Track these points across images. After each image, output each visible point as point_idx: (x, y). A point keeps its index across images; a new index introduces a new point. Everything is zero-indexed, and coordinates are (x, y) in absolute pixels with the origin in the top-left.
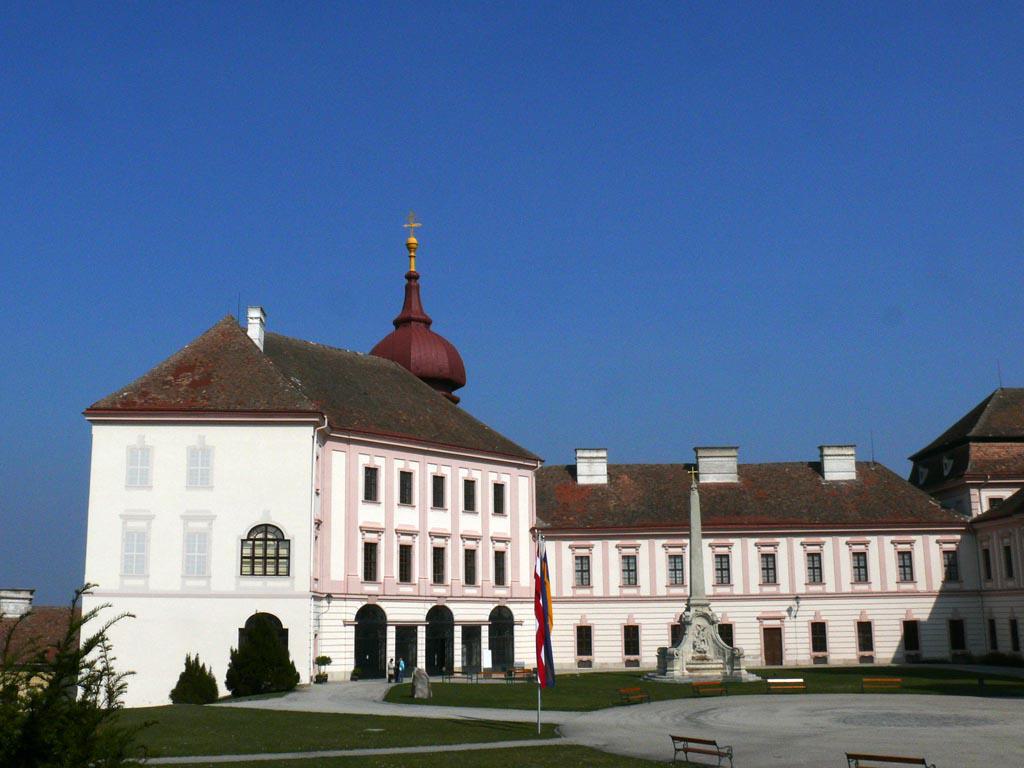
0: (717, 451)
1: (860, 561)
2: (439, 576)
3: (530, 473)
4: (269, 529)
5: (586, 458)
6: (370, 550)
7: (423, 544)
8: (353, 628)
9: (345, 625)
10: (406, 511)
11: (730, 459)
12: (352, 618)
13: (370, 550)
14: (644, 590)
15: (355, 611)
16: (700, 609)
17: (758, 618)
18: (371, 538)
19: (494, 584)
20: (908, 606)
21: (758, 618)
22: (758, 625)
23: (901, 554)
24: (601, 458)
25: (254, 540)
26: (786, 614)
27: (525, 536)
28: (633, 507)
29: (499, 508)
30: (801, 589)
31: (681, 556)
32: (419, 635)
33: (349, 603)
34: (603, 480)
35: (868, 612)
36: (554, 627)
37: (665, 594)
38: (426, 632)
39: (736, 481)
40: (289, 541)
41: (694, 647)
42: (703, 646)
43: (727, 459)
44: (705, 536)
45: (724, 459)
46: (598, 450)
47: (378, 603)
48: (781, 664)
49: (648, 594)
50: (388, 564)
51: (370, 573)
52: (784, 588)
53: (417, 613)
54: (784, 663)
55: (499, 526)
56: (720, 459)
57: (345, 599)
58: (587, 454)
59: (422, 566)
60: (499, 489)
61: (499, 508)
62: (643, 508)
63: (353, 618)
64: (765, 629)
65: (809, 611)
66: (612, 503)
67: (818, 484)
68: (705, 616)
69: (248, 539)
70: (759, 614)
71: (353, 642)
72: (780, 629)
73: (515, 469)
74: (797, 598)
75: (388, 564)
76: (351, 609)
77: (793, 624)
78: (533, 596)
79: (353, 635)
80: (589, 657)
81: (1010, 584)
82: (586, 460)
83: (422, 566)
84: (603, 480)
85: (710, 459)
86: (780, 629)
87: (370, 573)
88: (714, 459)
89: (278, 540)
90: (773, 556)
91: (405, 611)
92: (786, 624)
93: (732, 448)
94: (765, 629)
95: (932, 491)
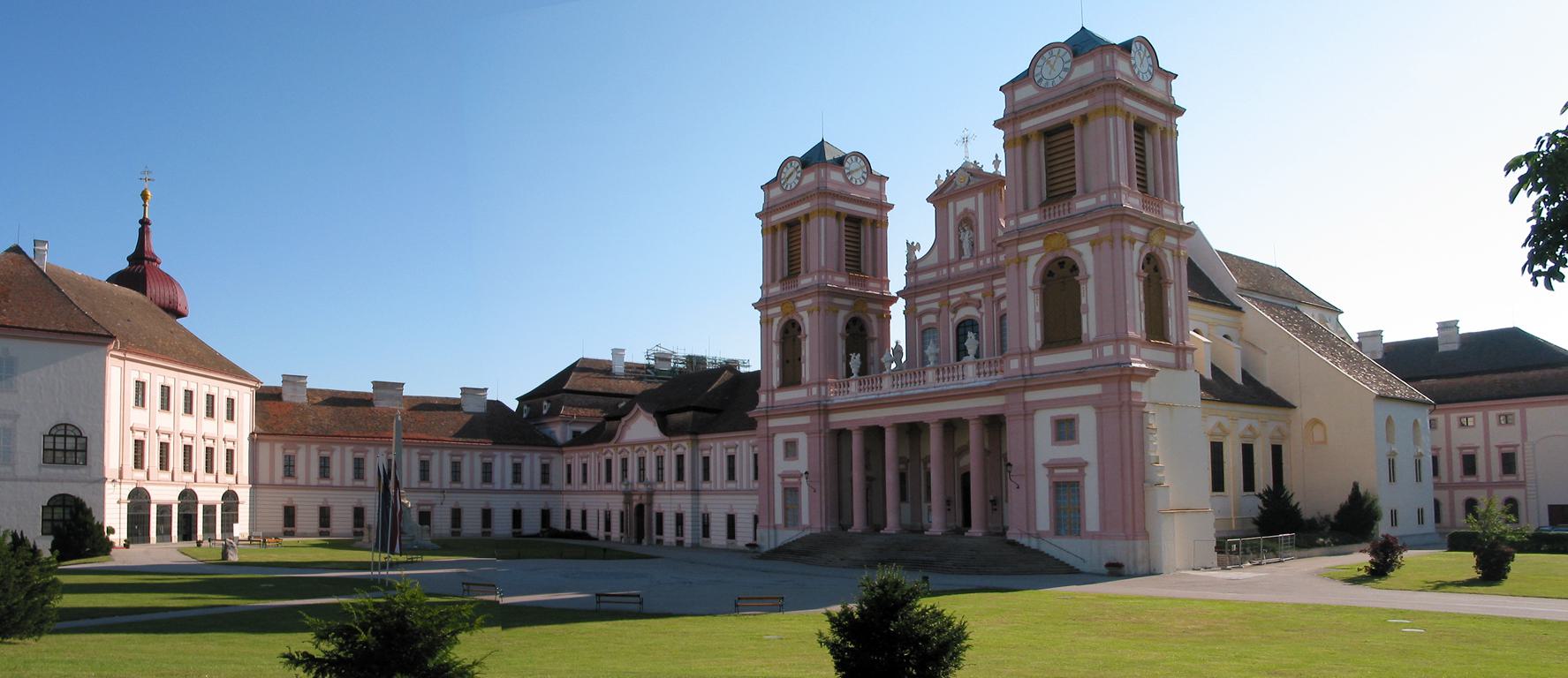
2: (187, 467)
4: (68, 427)
6: (139, 445)
10: (165, 415)
12: (125, 497)
13: (139, 445)
25: (55, 436)
29: (230, 416)
36: (299, 511)
40: (86, 438)
47: (144, 487)
49: (338, 485)
50: (152, 456)
51: (139, 463)
52: (435, 485)
55: (229, 429)
59: (176, 459)
60: (231, 402)
61: (230, 416)
65: (451, 501)
66: (311, 417)
69: (50, 435)
74: (443, 491)
75: (152, 456)
76: (127, 489)
80: (293, 529)
81: (584, 487)
83: (176, 459)
87: (139, 463)
89: (76, 437)
91: (164, 492)
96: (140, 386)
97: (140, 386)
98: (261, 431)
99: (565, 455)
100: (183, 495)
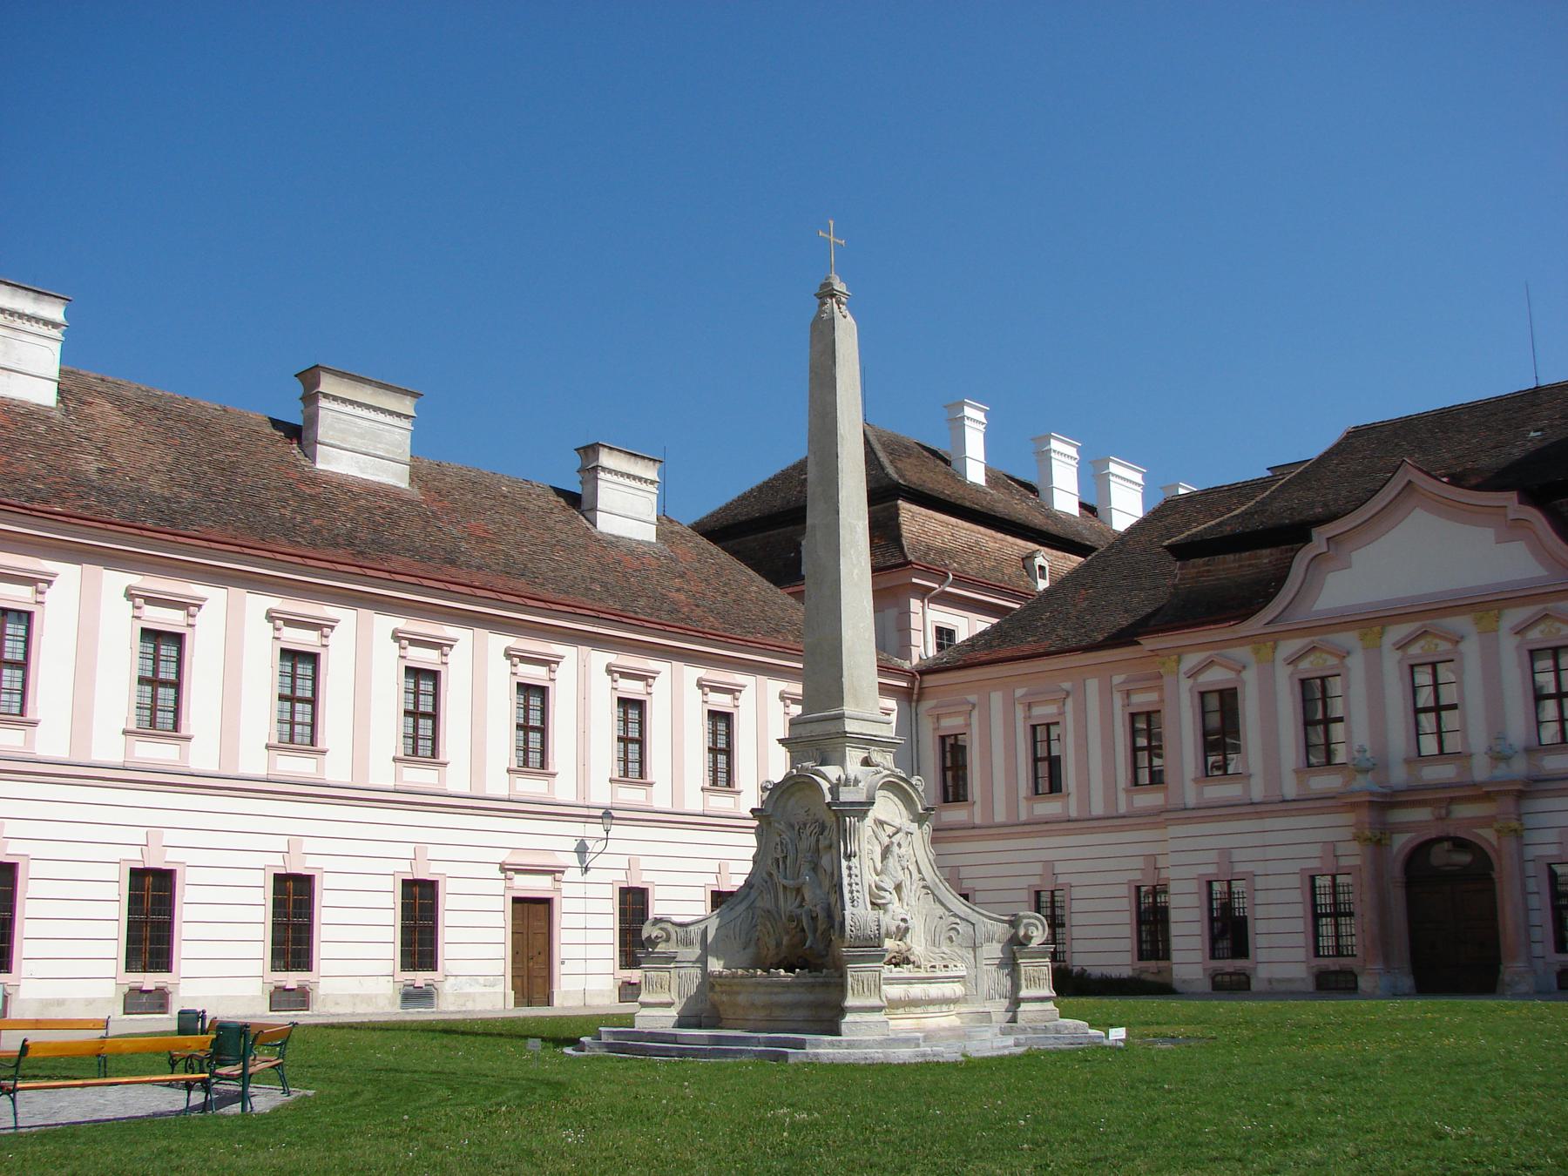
17: (503, 868)
21: (503, 868)
22: (500, 886)
24: (47, 323)
26: (573, 859)
34: (45, 395)
35: (645, 863)
37: (261, 772)
39: (404, 485)
45: (381, 417)
48: (548, 1002)
54: (557, 1001)
56: (372, 415)
62: (187, 495)
64: (516, 900)
72: (547, 902)
84: (45, 395)
85: (349, 409)
88: (359, 411)
92: (567, 890)
93: (406, 392)
94: (516, 900)
95: (791, 590)
99: (927, 704)
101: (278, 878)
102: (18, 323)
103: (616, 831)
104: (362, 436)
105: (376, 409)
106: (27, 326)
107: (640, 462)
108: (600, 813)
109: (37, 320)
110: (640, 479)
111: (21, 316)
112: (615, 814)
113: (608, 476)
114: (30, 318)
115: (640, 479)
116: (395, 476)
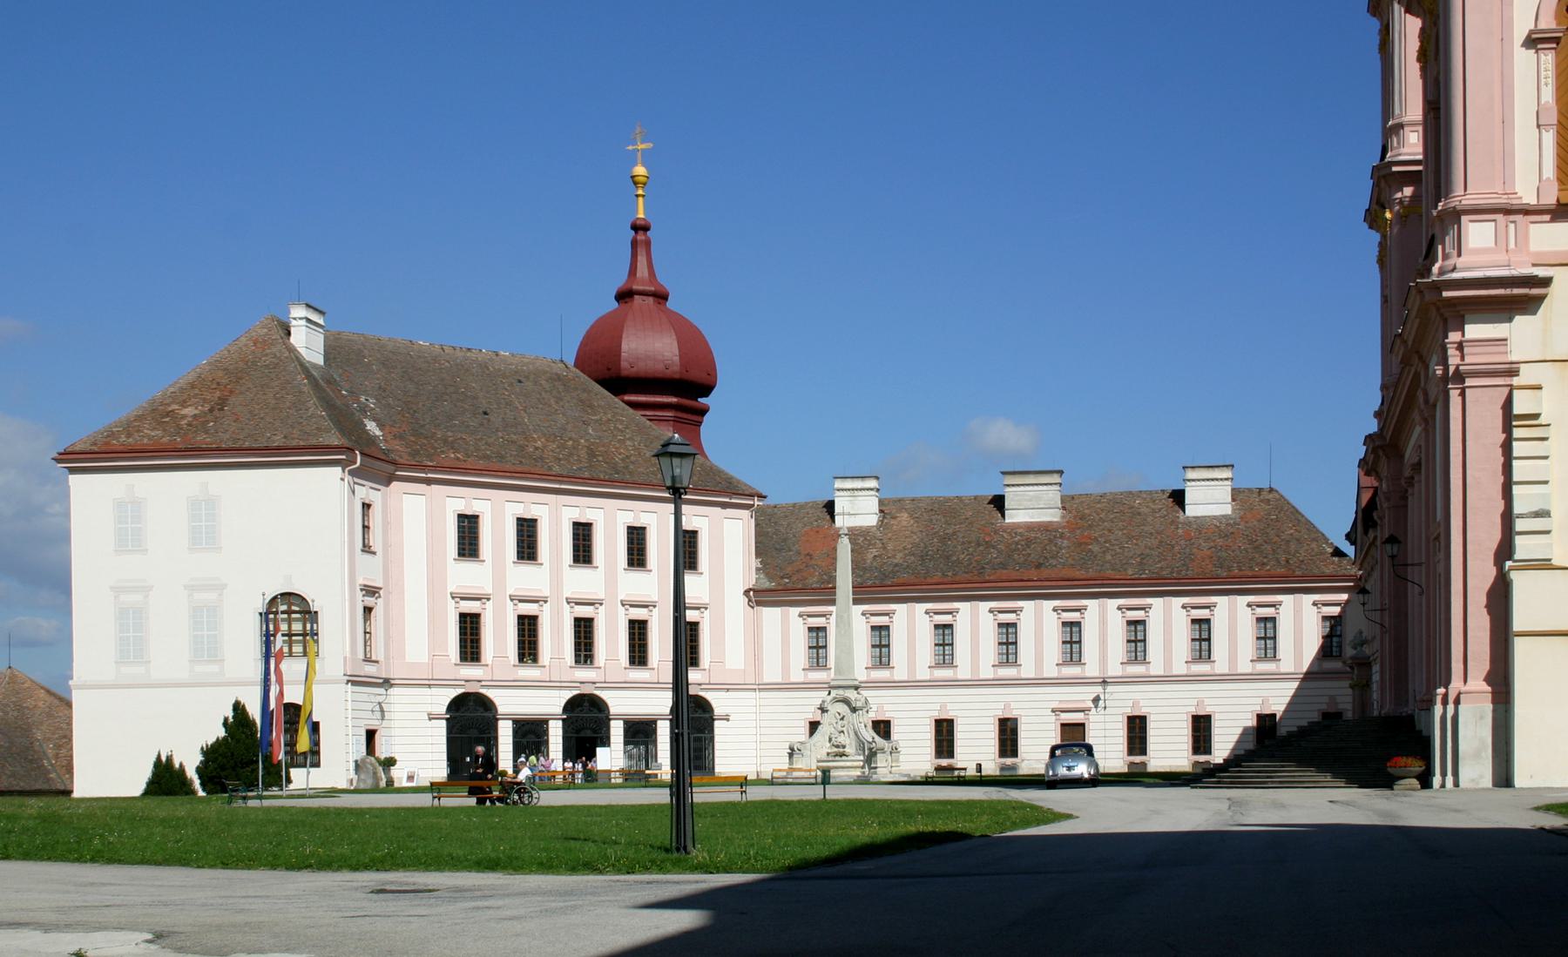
0: (1032, 476)
1: (1202, 631)
3: (745, 513)
5: (846, 490)
7: (558, 615)
8: (444, 723)
9: (430, 719)
11: (1049, 487)
12: (441, 708)
13: (470, 627)
14: (963, 671)
15: (448, 701)
16: (841, 692)
18: (470, 607)
19: (628, 665)
20: (1265, 693)
21: (1053, 711)
23: (1262, 620)
26: (1091, 705)
27: (736, 603)
28: (898, 559)
30: (1115, 669)
31: (1080, 623)
32: (551, 731)
33: (434, 690)
38: (564, 728)
41: (830, 740)
42: (842, 739)
43: (1045, 488)
44: (856, 602)
45: (1041, 488)
46: (863, 478)
50: (499, 639)
53: (549, 704)
56: (1036, 488)
57: (430, 686)
58: (849, 484)
59: (556, 640)
63: (443, 710)
64: (1062, 725)
65: (1124, 702)
67: (1174, 522)
68: (846, 701)
70: (1056, 705)
71: (444, 740)
72: (1083, 725)
73: (718, 510)
74: (1104, 683)
75: (499, 639)
76: (442, 699)
77: (1101, 718)
78: (670, 679)
79: (444, 732)
82: (848, 493)
83: (556, 640)
85: (1022, 488)
86: (1083, 725)
90: (1273, 620)
94: (1062, 725)
96: (468, 529)
97: (468, 529)
98: (767, 584)
100: (573, 705)
101: (1129, 718)
102: (856, 493)
103: (1110, 688)
104: (1030, 500)
105: (1037, 484)
106: (860, 493)
107: (1216, 469)
108: (1101, 680)
109: (864, 489)
110: (1217, 480)
111: (857, 490)
112: (1108, 680)
113: (1193, 483)
114: (861, 490)
115: (1217, 480)
116: (1053, 516)
